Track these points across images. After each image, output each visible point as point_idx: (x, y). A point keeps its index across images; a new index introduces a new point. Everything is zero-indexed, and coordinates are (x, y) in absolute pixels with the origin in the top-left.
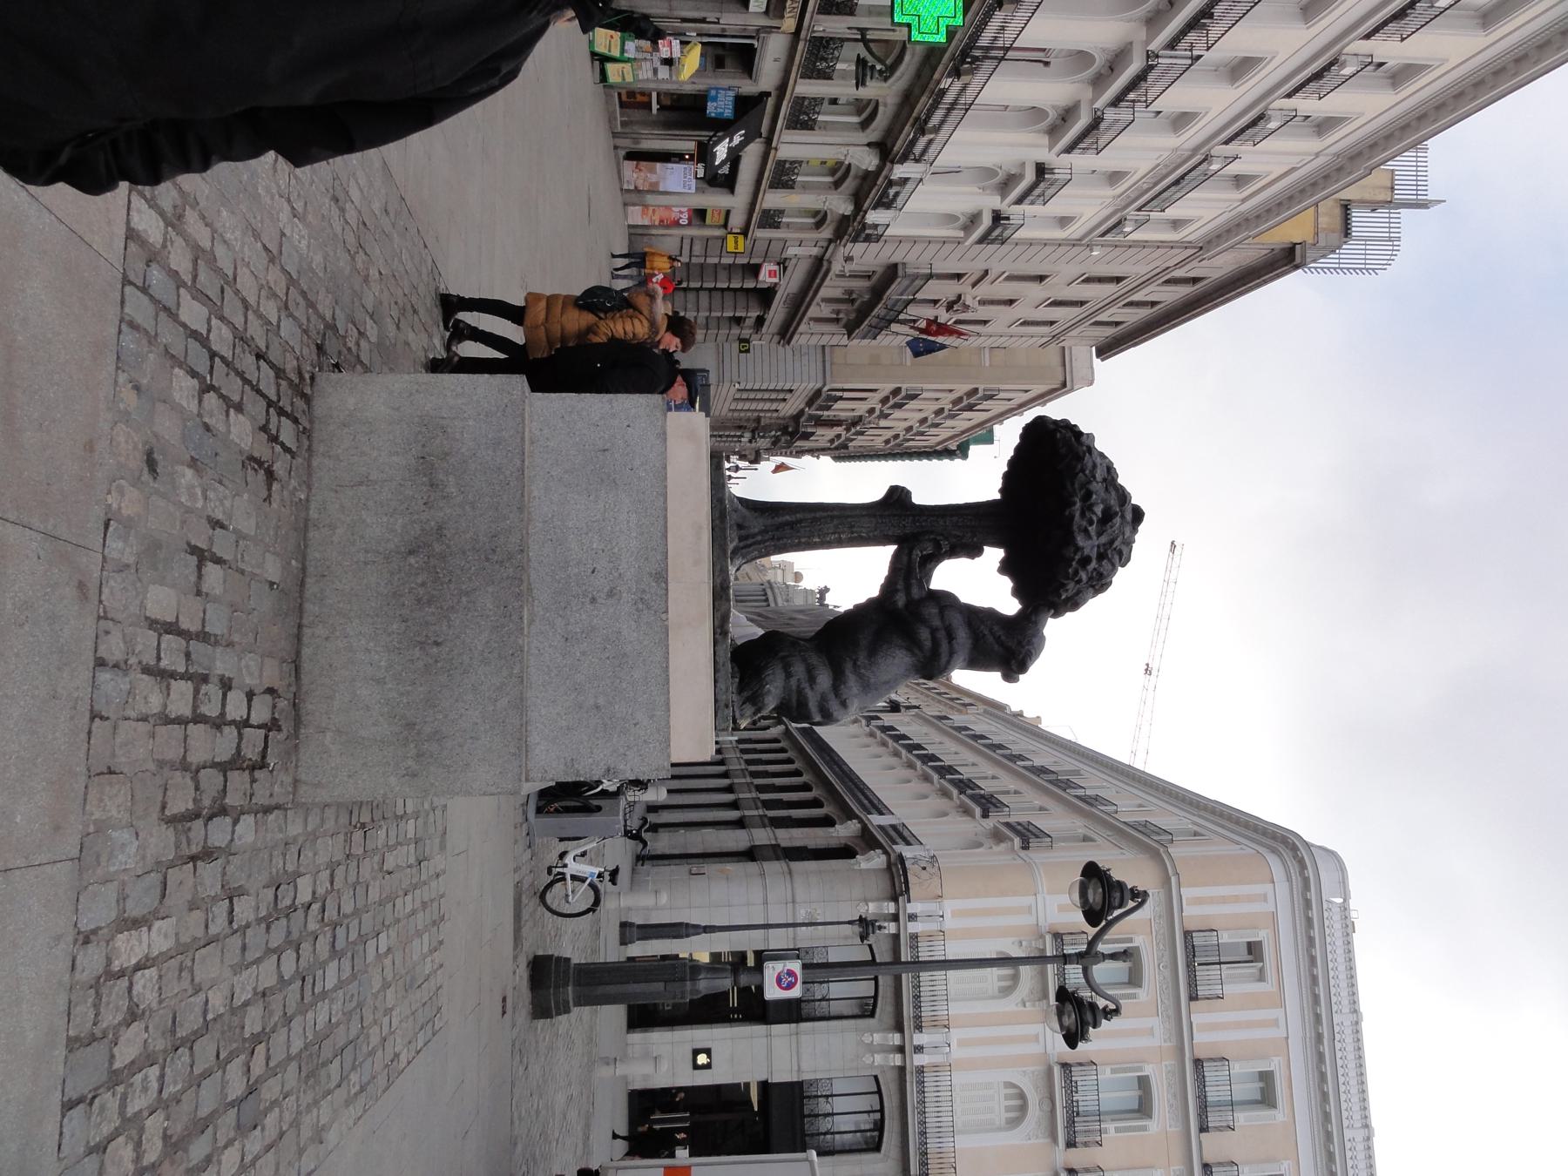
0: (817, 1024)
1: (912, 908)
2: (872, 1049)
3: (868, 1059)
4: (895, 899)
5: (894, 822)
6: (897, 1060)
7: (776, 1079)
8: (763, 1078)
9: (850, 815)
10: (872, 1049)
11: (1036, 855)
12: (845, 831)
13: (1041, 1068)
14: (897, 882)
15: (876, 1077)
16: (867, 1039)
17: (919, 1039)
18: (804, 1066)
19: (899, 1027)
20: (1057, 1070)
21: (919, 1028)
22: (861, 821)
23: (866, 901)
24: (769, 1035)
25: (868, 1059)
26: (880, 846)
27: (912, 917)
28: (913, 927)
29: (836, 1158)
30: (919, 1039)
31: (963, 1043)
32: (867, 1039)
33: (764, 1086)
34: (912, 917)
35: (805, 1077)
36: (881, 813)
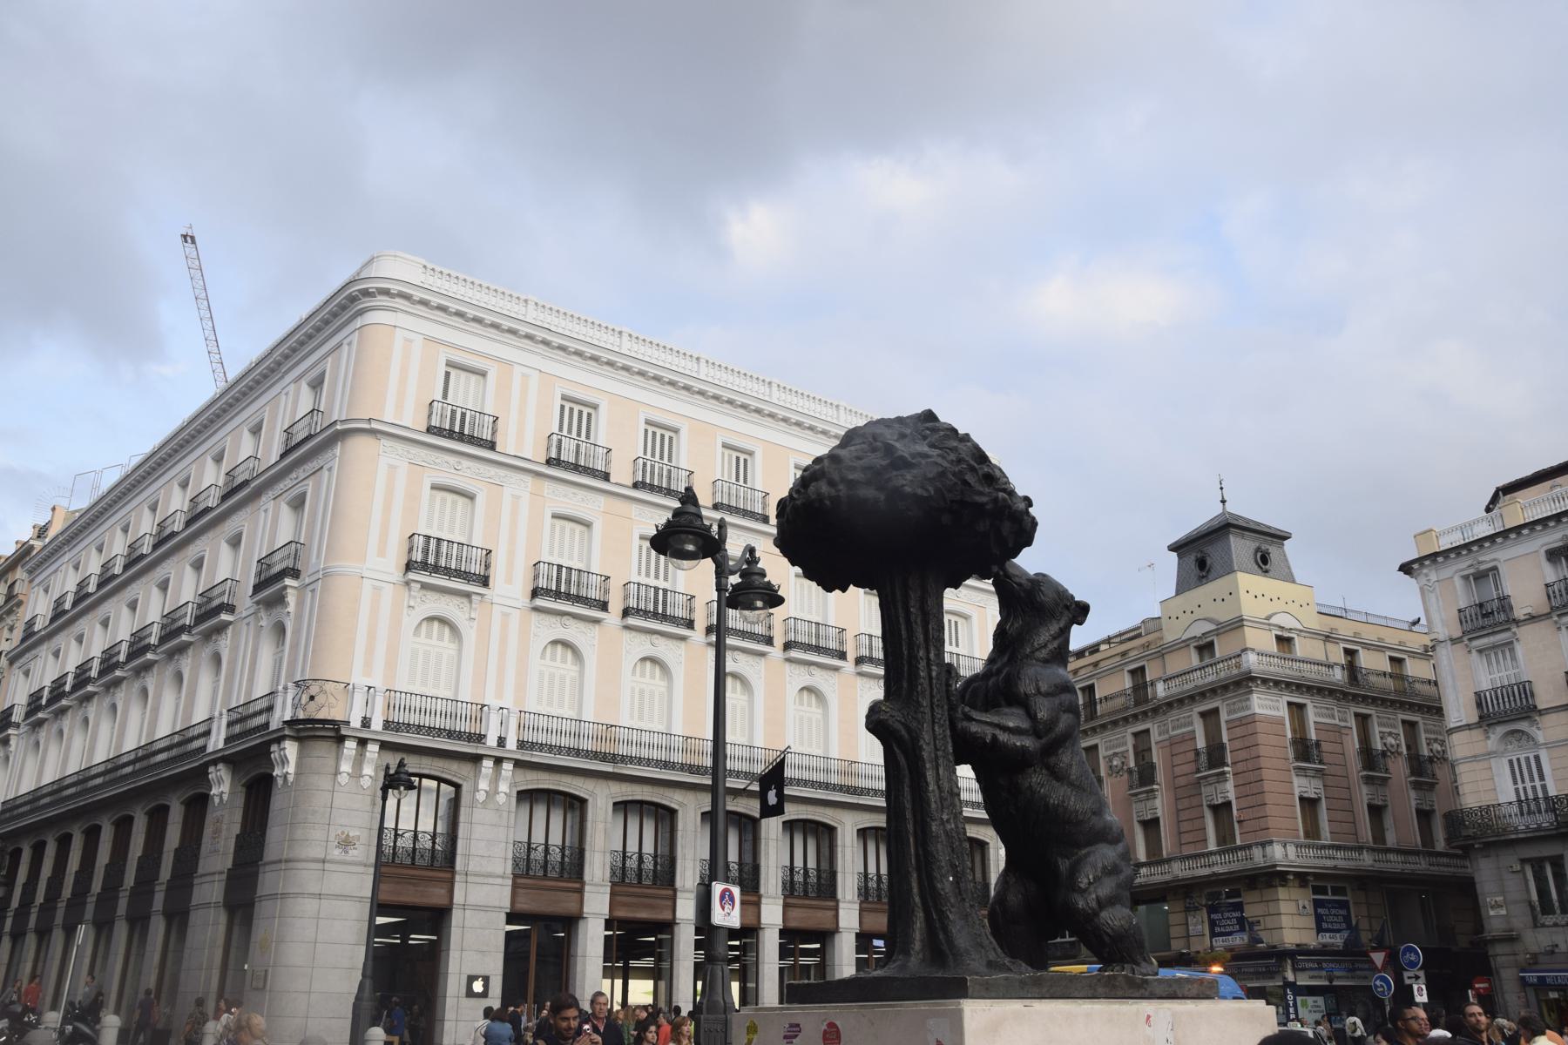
0: (460, 850)
1: (356, 723)
2: (492, 793)
3: (501, 799)
4: (341, 740)
5: (224, 722)
6: (508, 767)
7: (506, 903)
8: (503, 917)
9: (201, 774)
10: (492, 793)
11: (312, 563)
12: (222, 785)
13: (535, 616)
14: (319, 732)
15: (519, 793)
16: (481, 796)
17: (492, 741)
18: (499, 871)
19: (476, 759)
20: (539, 602)
21: (480, 738)
22: (215, 762)
23: (337, 773)
24: (464, 907)
25: (501, 799)
26: (269, 743)
27: (366, 723)
28: (377, 725)
29: (587, 847)
30: (492, 741)
31: (499, 693)
32: (481, 796)
33: (511, 918)
34: (366, 723)
35: (509, 870)
36: (207, 733)
